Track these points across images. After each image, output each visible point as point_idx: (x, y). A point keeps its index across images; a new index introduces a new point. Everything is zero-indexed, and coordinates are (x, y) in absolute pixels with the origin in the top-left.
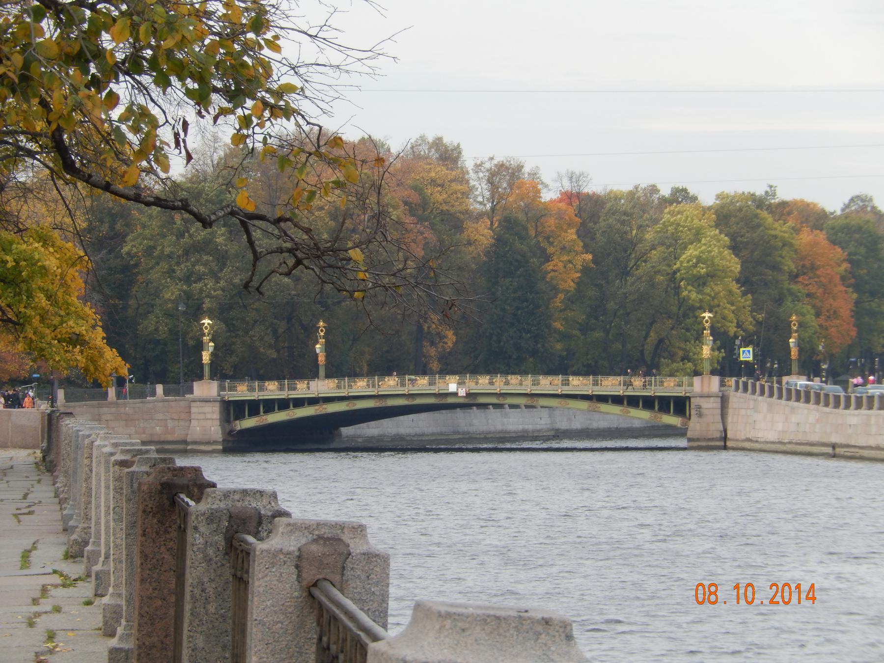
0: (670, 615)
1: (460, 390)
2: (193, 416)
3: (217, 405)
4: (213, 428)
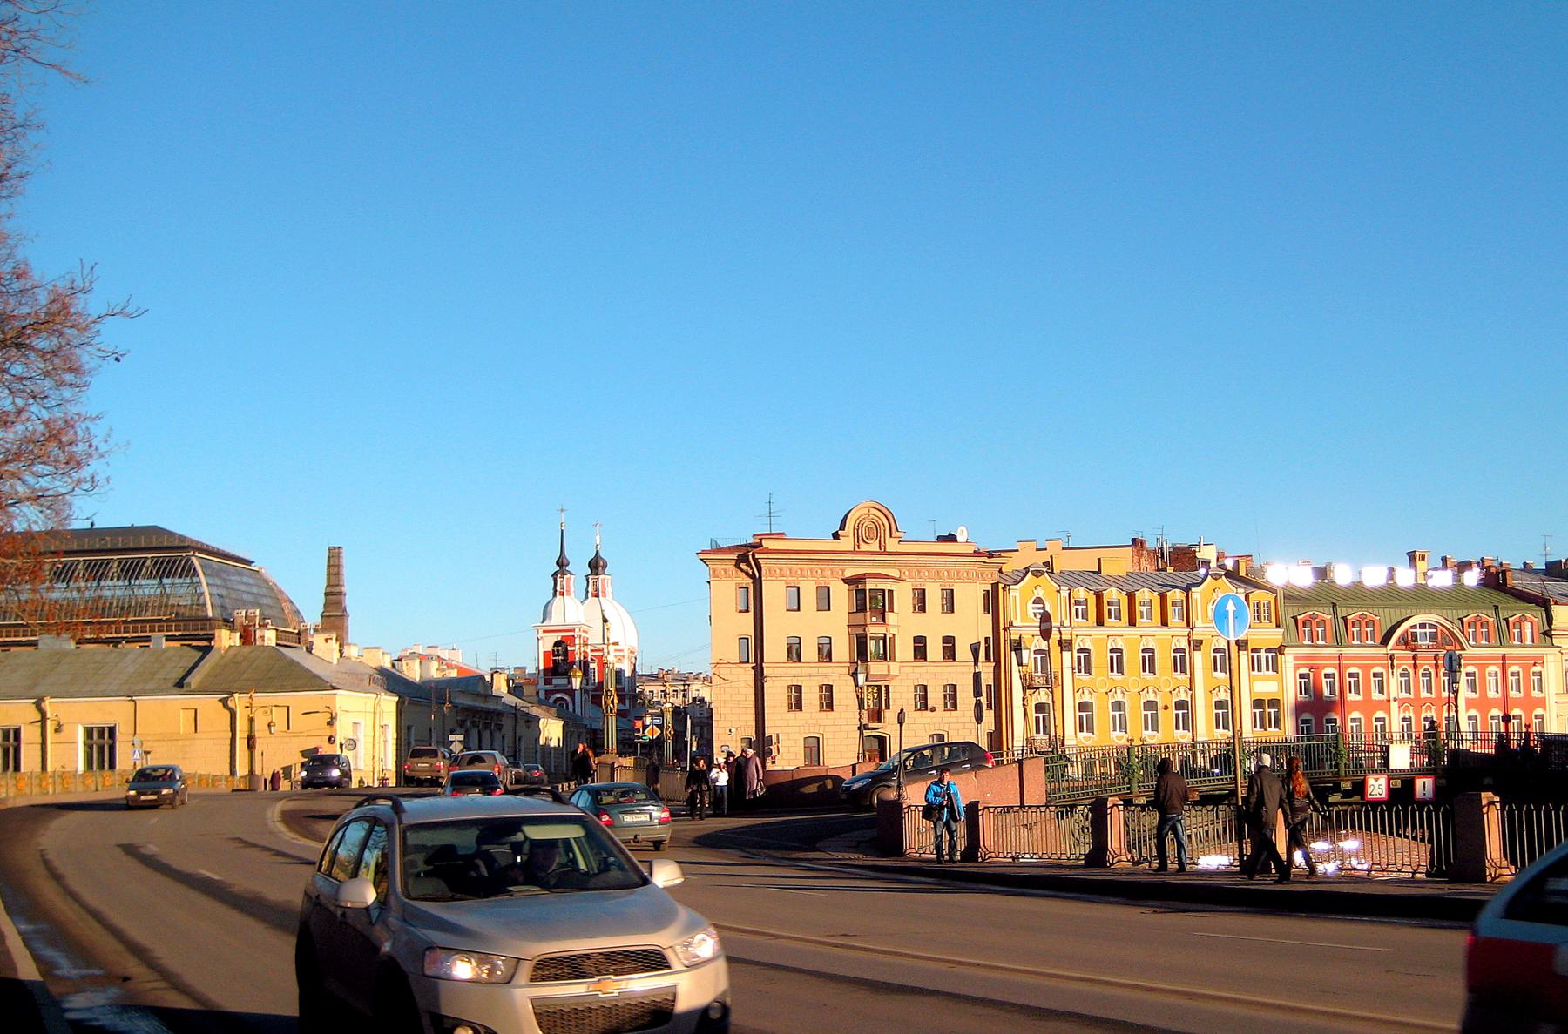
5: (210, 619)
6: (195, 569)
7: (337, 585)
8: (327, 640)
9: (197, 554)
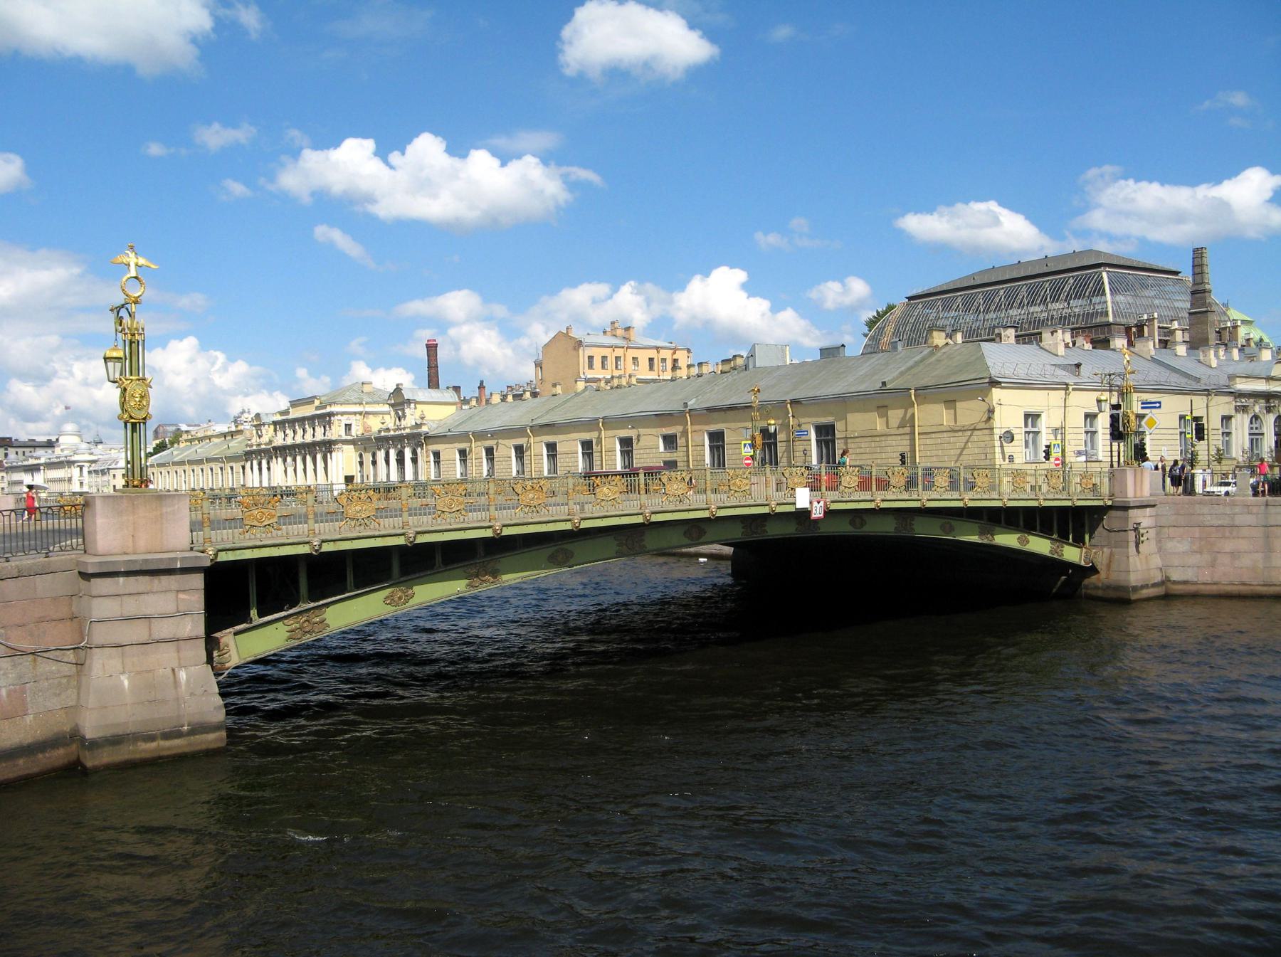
0: (1201, 929)
1: (815, 504)
2: (100, 634)
3: (198, 581)
4: (183, 675)
5: (1111, 324)
6: (1103, 283)
7: (1201, 284)
8: (1052, 333)
9: (1107, 269)
